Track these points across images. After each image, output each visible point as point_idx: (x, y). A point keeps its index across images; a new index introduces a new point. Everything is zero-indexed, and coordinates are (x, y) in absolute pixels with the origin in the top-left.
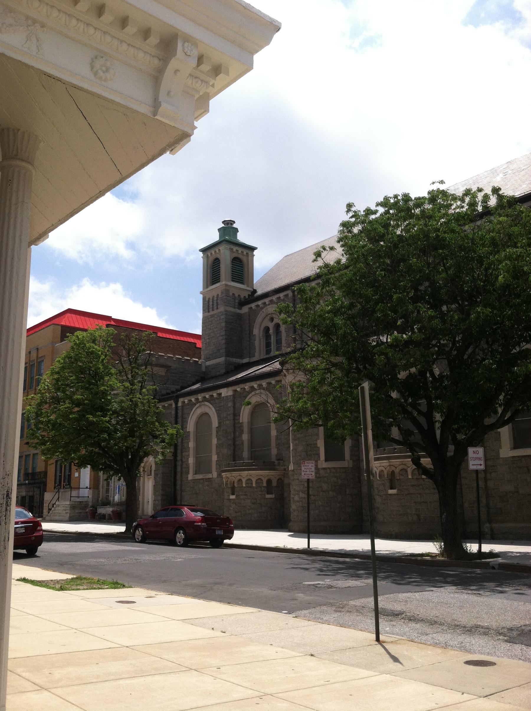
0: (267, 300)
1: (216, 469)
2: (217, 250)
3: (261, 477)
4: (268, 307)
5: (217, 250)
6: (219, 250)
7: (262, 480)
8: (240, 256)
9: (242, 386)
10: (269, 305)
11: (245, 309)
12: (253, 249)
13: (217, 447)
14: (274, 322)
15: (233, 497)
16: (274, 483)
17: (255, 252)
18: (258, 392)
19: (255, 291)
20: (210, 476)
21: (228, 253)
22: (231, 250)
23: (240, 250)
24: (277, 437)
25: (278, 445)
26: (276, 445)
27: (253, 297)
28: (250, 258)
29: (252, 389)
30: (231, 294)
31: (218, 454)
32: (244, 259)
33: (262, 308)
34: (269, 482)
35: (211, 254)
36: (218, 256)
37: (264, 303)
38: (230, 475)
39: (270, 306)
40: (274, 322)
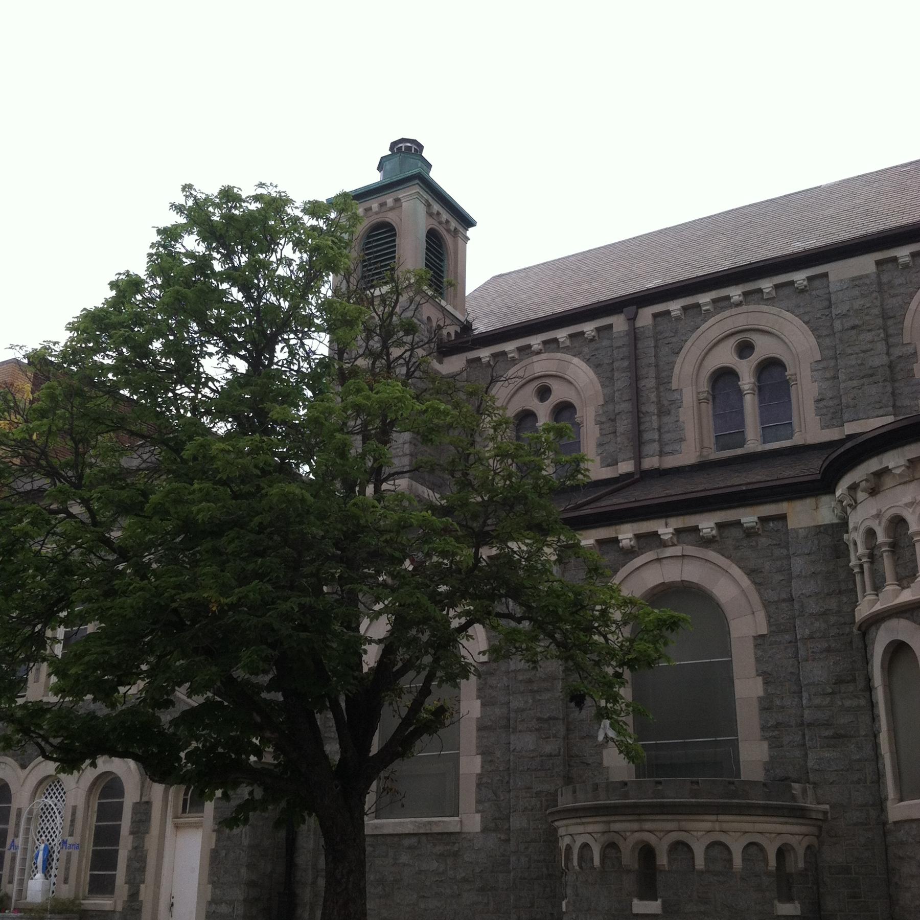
0: (535, 341)
1: (479, 802)
2: (390, 201)
3: (758, 839)
4: (535, 358)
5: (390, 201)
6: (397, 200)
7: (727, 848)
8: (442, 230)
9: (604, 533)
10: (539, 353)
11: (454, 365)
12: (468, 222)
13: (481, 728)
14: (553, 400)
15: (653, 907)
16: (797, 863)
17: (471, 232)
18: (669, 551)
19: (467, 327)
20: (450, 823)
21: (421, 209)
22: (429, 205)
23: (445, 216)
24: (766, 705)
25: (773, 732)
26: (763, 728)
27: (466, 339)
28: (460, 241)
29: (650, 540)
30: (425, 318)
31: (485, 752)
32: (448, 239)
33: (514, 361)
34: (781, 853)
35: (368, 210)
36: (391, 217)
37: (525, 350)
38: (635, 826)
39: (544, 356)
40: (553, 400)
